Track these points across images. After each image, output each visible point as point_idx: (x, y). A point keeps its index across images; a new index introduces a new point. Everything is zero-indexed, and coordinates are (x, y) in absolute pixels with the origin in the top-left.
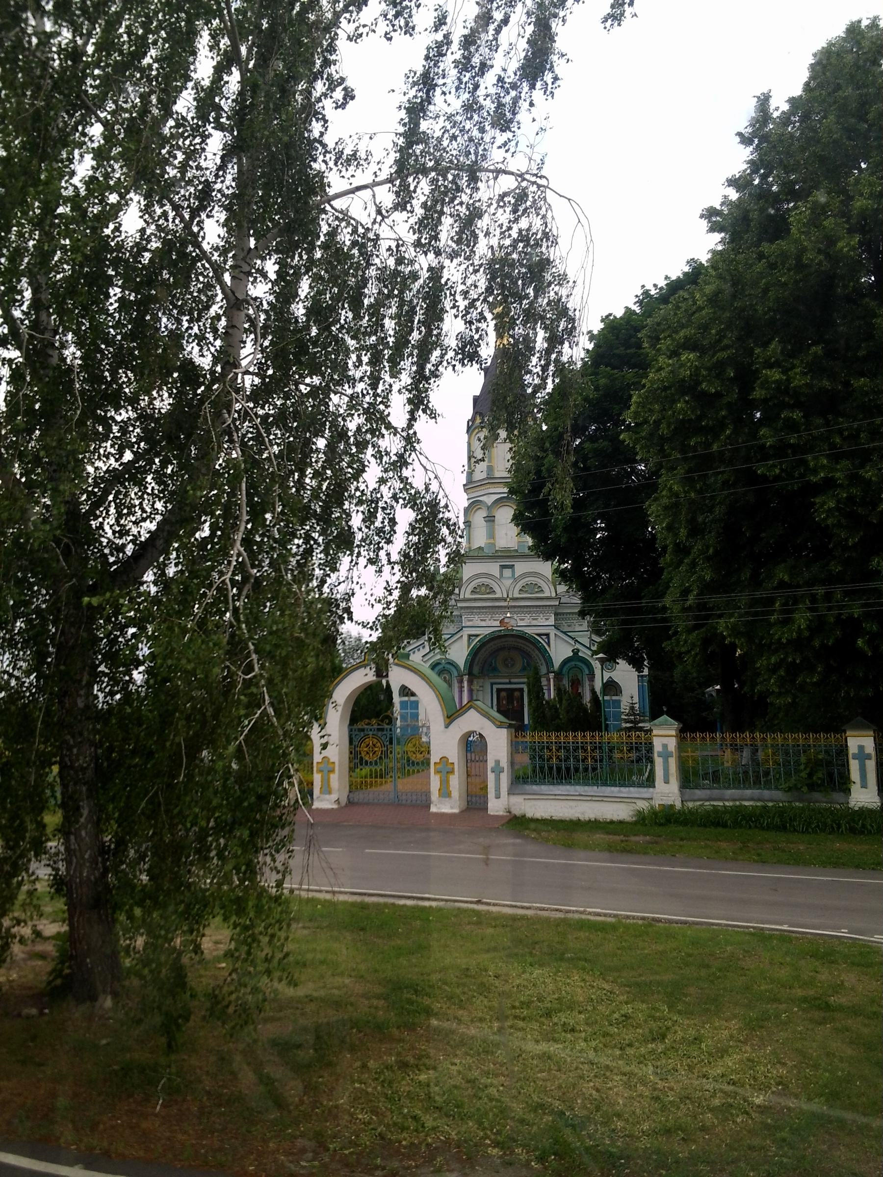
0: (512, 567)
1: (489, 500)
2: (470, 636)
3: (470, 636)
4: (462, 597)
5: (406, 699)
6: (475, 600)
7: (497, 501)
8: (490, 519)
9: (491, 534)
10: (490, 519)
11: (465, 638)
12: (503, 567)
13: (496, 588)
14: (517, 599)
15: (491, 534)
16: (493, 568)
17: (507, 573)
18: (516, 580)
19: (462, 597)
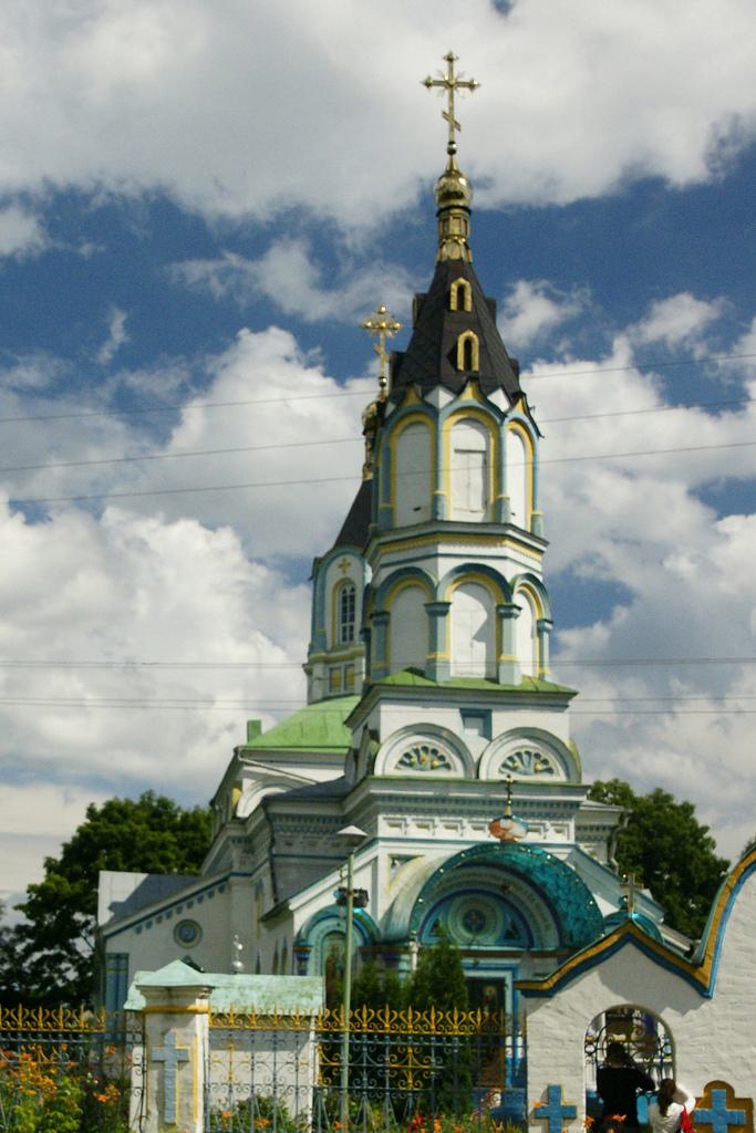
11: (384, 863)
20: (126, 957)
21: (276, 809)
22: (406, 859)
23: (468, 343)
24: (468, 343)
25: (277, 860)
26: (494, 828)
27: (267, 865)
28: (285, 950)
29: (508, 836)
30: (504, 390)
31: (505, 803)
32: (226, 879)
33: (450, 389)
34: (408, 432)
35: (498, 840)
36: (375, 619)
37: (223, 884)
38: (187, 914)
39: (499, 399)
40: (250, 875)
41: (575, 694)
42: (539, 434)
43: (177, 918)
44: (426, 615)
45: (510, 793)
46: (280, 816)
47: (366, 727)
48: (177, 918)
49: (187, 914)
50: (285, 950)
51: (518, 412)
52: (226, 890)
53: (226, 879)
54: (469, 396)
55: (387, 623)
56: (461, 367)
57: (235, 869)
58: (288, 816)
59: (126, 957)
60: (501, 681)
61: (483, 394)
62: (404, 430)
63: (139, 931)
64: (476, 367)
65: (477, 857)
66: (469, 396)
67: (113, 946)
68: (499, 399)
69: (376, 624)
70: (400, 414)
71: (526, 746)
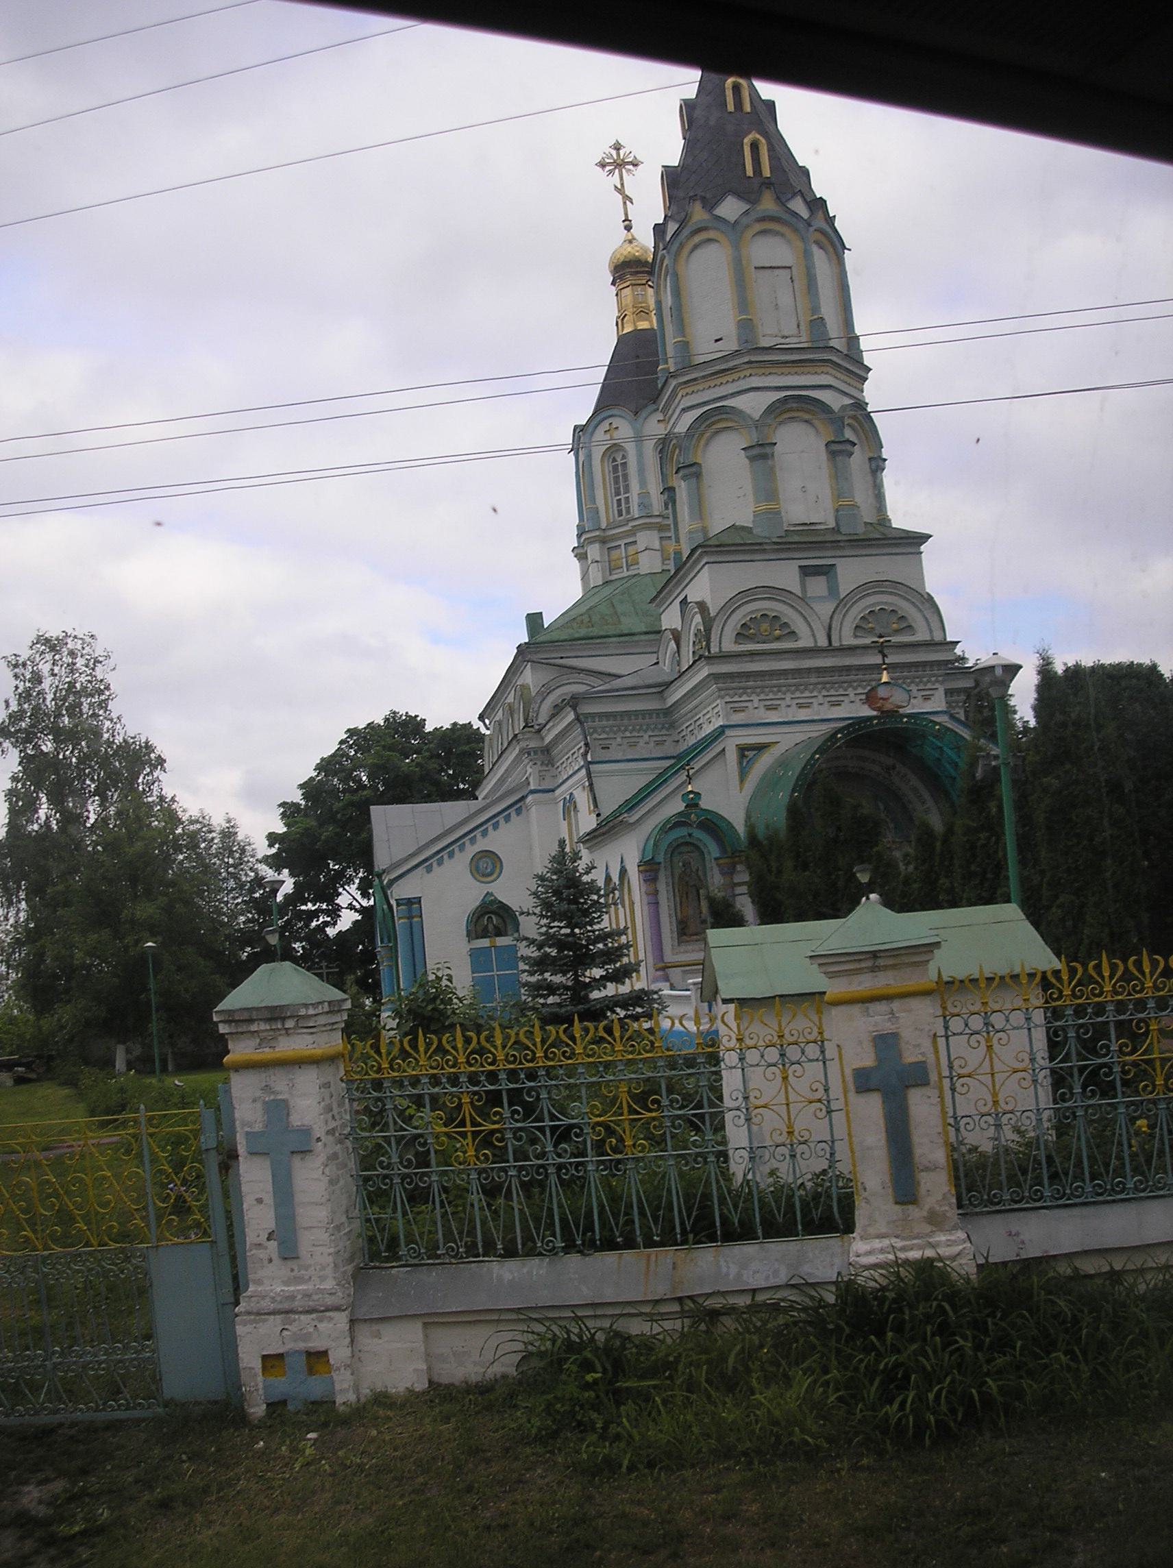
0: (826, 571)
1: (754, 405)
2: (742, 750)
3: (742, 750)
4: (714, 649)
5: (485, 943)
6: (752, 654)
7: (772, 409)
8: (761, 453)
9: (767, 490)
10: (761, 453)
11: (732, 756)
12: (806, 571)
13: (799, 625)
14: (852, 649)
15: (767, 490)
16: (785, 574)
17: (818, 586)
18: (843, 604)
19: (714, 649)
20: (418, 900)
21: (586, 709)
22: (761, 748)
23: (755, 146)
24: (755, 146)
25: (593, 767)
26: (870, 699)
27: (584, 771)
28: (623, 872)
29: (888, 706)
30: (803, 196)
31: (877, 668)
32: (523, 798)
33: (740, 196)
34: (698, 253)
35: (875, 713)
36: (681, 474)
37: (518, 806)
38: (482, 844)
39: (798, 206)
40: (553, 791)
41: (925, 538)
42: (844, 248)
43: (471, 850)
44: (747, 461)
45: (884, 656)
46: (593, 716)
47: (684, 602)
48: (471, 850)
49: (482, 844)
50: (623, 872)
51: (820, 222)
52: (524, 812)
53: (523, 798)
54: (768, 204)
55: (698, 476)
56: (750, 172)
57: (532, 787)
58: (601, 716)
59: (418, 900)
60: (843, 530)
61: (781, 201)
62: (692, 251)
63: (429, 870)
64: (767, 172)
65: (857, 736)
66: (768, 204)
67: (402, 891)
68: (798, 206)
69: (684, 478)
70: (686, 232)
71: (878, 603)
